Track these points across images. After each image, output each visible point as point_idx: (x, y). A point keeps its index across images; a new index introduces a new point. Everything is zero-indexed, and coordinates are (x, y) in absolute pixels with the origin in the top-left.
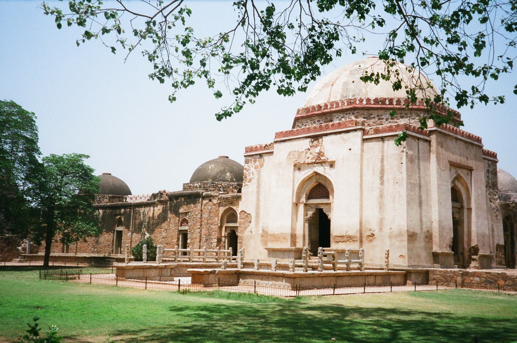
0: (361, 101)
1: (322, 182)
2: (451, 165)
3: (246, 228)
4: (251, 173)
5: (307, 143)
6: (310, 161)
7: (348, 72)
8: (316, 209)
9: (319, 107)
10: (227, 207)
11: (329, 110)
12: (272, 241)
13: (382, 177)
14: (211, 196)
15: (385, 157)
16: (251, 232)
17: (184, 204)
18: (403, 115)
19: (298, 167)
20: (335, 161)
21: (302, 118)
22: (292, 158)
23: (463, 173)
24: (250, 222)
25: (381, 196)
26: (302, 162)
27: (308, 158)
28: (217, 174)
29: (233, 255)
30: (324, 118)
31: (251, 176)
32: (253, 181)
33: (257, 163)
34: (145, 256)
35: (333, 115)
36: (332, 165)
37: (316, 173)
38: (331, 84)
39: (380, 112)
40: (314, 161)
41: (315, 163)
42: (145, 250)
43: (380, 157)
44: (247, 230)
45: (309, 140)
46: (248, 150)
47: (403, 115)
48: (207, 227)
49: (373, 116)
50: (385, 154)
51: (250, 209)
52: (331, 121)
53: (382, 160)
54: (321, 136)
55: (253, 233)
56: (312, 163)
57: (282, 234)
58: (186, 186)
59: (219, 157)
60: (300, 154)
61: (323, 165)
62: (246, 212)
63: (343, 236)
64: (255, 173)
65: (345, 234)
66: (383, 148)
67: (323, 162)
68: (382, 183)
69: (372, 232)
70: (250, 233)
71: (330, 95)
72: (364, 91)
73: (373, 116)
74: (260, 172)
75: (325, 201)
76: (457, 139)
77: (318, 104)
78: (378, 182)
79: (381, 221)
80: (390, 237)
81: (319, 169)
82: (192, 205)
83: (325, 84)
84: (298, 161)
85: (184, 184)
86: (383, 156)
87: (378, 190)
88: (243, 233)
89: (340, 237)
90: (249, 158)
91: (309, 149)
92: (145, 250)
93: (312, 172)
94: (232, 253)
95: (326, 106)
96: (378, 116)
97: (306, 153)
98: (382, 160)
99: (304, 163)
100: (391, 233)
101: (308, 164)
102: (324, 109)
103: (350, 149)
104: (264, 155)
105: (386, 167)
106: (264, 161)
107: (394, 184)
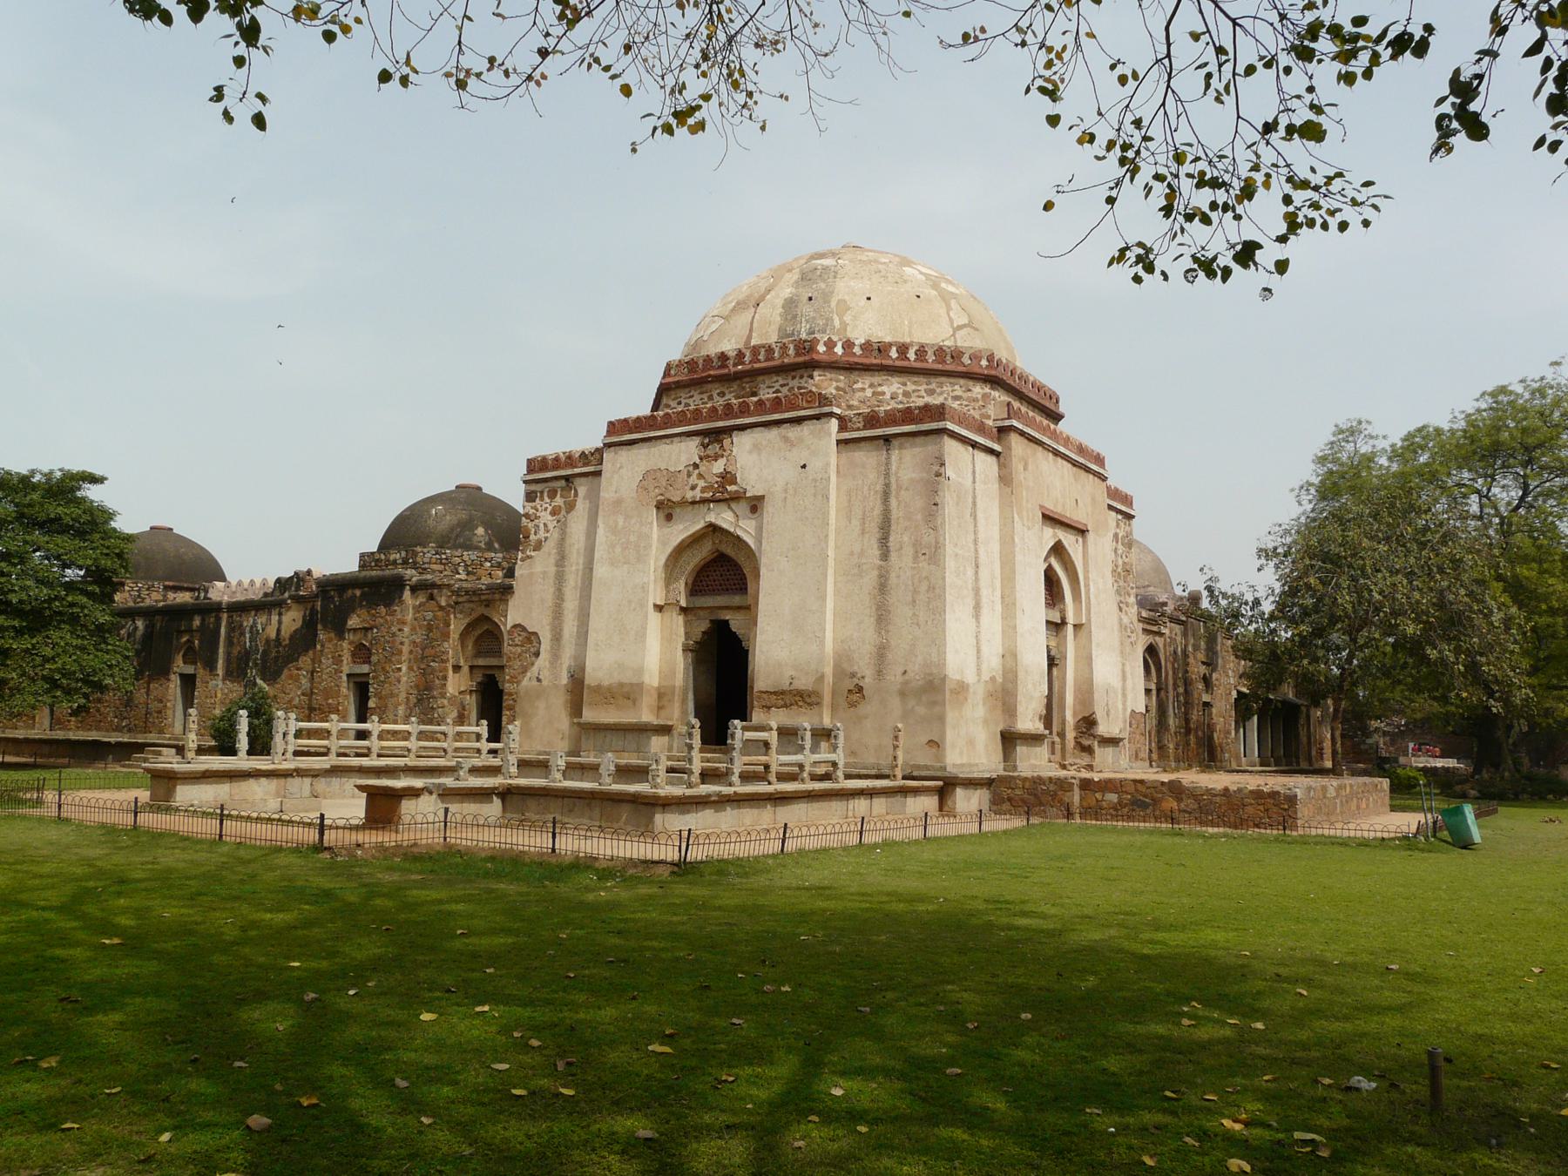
0: (830, 344)
1: (729, 551)
2: (1044, 516)
5: (689, 450)
6: (698, 494)
7: (795, 276)
9: (723, 357)
10: (475, 615)
11: (748, 367)
14: (433, 585)
15: (894, 486)
16: (539, 680)
17: (361, 606)
18: (933, 386)
20: (763, 497)
21: (679, 385)
23: (1068, 540)
24: (537, 654)
25: (883, 587)
26: (676, 499)
27: (693, 488)
28: (452, 529)
29: (489, 740)
30: (735, 386)
31: (542, 534)
32: (546, 547)
33: (559, 501)
34: (243, 743)
35: (760, 378)
36: (755, 505)
37: (713, 529)
38: (753, 302)
39: (877, 379)
40: (708, 495)
42: (243, 726)
43: (879, 487)
45: (696, 441)
46: (535, 465)
47: (933, 386)
49: (859, 385)
50: (893, 480)
51: (539, 623)
52: (754, 394)
53: (886, 496)
54: (729, 431)
55: (545, 683)
56: (704, 501)
57: (621, 685)
58: (366, 560)
60: (672, 477)
61: (733, 505)
62: (524, 629)
63: (783, 693)
64: (551, 527)
65: (786, 687)
66: (888, 464)
67: (732, 499)
68: (885, 556)
69: (856, 681)
70: (535, 683)
72: (837, 323)
73: (859, 385)
74: (565, 524)
75: (737, 600)
76: (1056, 453)
77: (719, 350)
78: (875, 552)
79: (881, 652)
80: (903, 694)
81: (724, 518)
82: (383, 610)
83: (738, 303)
84: (668, 495)
85: (362, 555)
86: (887, 485)
87: (876, 573)
88: (518, 683)
89: (775, 693)
90: (533, 487)
91: (696, 466)
92: (243, 726)
93: (701, 525)
94: (485, 735)
95: (740, 355)
96: (871, 386)
97: (689, 475)
98: (886, 496)
99: (684, 503)
100: (906, 683)
101: (693, 503)
102: (735, 365)
103: (804, 467)
104: (577, 481)
106: (576, 495)
107: (915, 558)
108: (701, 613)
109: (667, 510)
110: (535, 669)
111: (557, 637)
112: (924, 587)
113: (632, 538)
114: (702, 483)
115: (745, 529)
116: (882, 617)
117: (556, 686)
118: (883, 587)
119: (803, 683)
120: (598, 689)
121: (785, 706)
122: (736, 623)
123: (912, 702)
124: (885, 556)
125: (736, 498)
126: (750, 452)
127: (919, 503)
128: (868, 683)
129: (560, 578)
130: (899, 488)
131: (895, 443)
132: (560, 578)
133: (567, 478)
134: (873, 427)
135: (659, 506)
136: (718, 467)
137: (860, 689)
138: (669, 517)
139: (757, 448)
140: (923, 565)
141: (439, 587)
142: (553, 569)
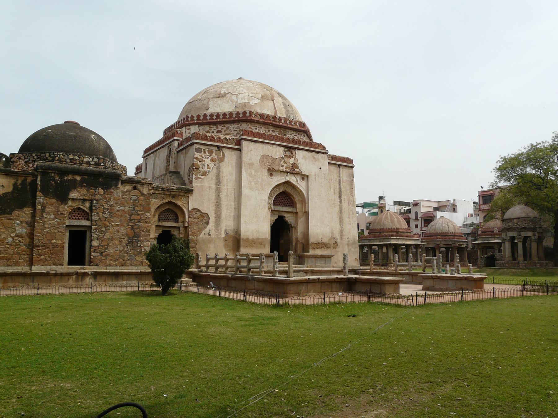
1: (289, 190)
3: (200, 230)
4: (206, 165)
8: (279, 216)
10: (165, 201)
12: (246, 246)
13: (340, 197)
16: (209, 235)
17: (82, 187)
19: (271, 172)
20: (307, 176)
22: (265, 162)
24: (208, 223)
25: (341, 211)
26: (276, 169)
27: (282, 166)
30: (278, 129)
31: (206, 169)
33: (214, 156)
36: (305, 177)
41: (288, 172)
43: (338, 180)
44: (203, 232)
45: (283, 149)
48: (131, 224)
51: (208, 208)
52: (285, 135)
54: (295, 149)
55: (213, 236)
57: (258, 239)
59: (65, 122)
60: (274, 160)
62: (199, 211)
63: (319, 243)
65: (320, 242)
68: (341, 202)
70: (207, 236)
71: (275, 109)
79: (342, 232)
80: (348, 245)
81: (292, 179)
82: (101, 191)
84: (272, 166)
86: (340, 180)
87: (338, 207)
91: (283, 158)
97: (281, 161)
100: (349, 241)
105: (343, 189)
108: (275, 213)
109: (271, 172)
110: (207, 230)
111: (218, 216)
112: (351, 213)
113: (259, 180)
114: (285, 165)
115: (301, 185)
116: (341, 221)
117: (219, 238)
118: (341, 211)
119: (325, 240)
120: (247, 240)
121: (320, 248)
122: (289, 218)
123: (350, 247)
124: (341, 202)
125: (297, 174)
126: (302, 158)
127: (348, 188)
128: (338, 241)
129: (218, 191)
130: (343, 182)
131: (341, 167)
132: (218, 191)
133: (219, 147)
134: (335, 161)
135: (269, 170)
136: (292, 161)
137: (336, 243)
138: (271, 175)
139: (304, 157)
140: (351, 206)
141: (143, 184)
142: (214, 186)
